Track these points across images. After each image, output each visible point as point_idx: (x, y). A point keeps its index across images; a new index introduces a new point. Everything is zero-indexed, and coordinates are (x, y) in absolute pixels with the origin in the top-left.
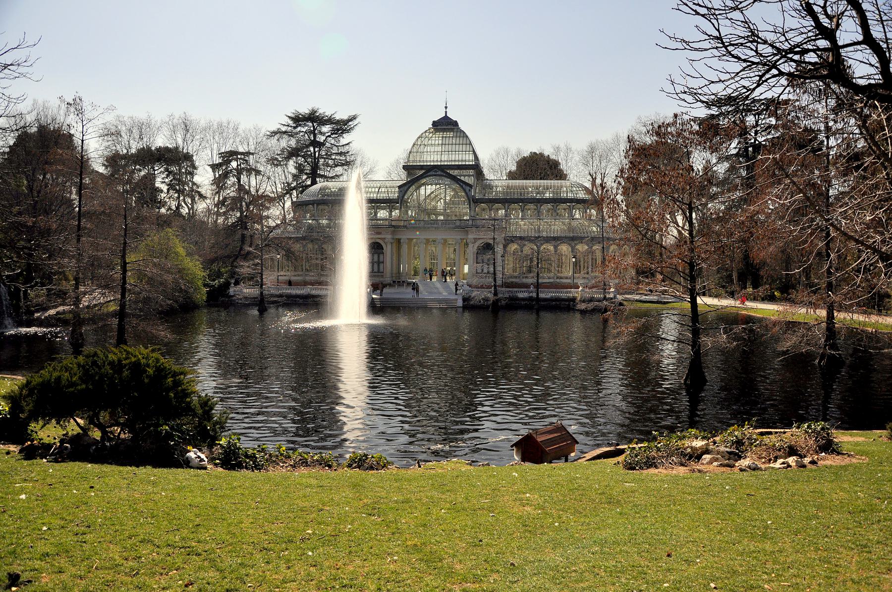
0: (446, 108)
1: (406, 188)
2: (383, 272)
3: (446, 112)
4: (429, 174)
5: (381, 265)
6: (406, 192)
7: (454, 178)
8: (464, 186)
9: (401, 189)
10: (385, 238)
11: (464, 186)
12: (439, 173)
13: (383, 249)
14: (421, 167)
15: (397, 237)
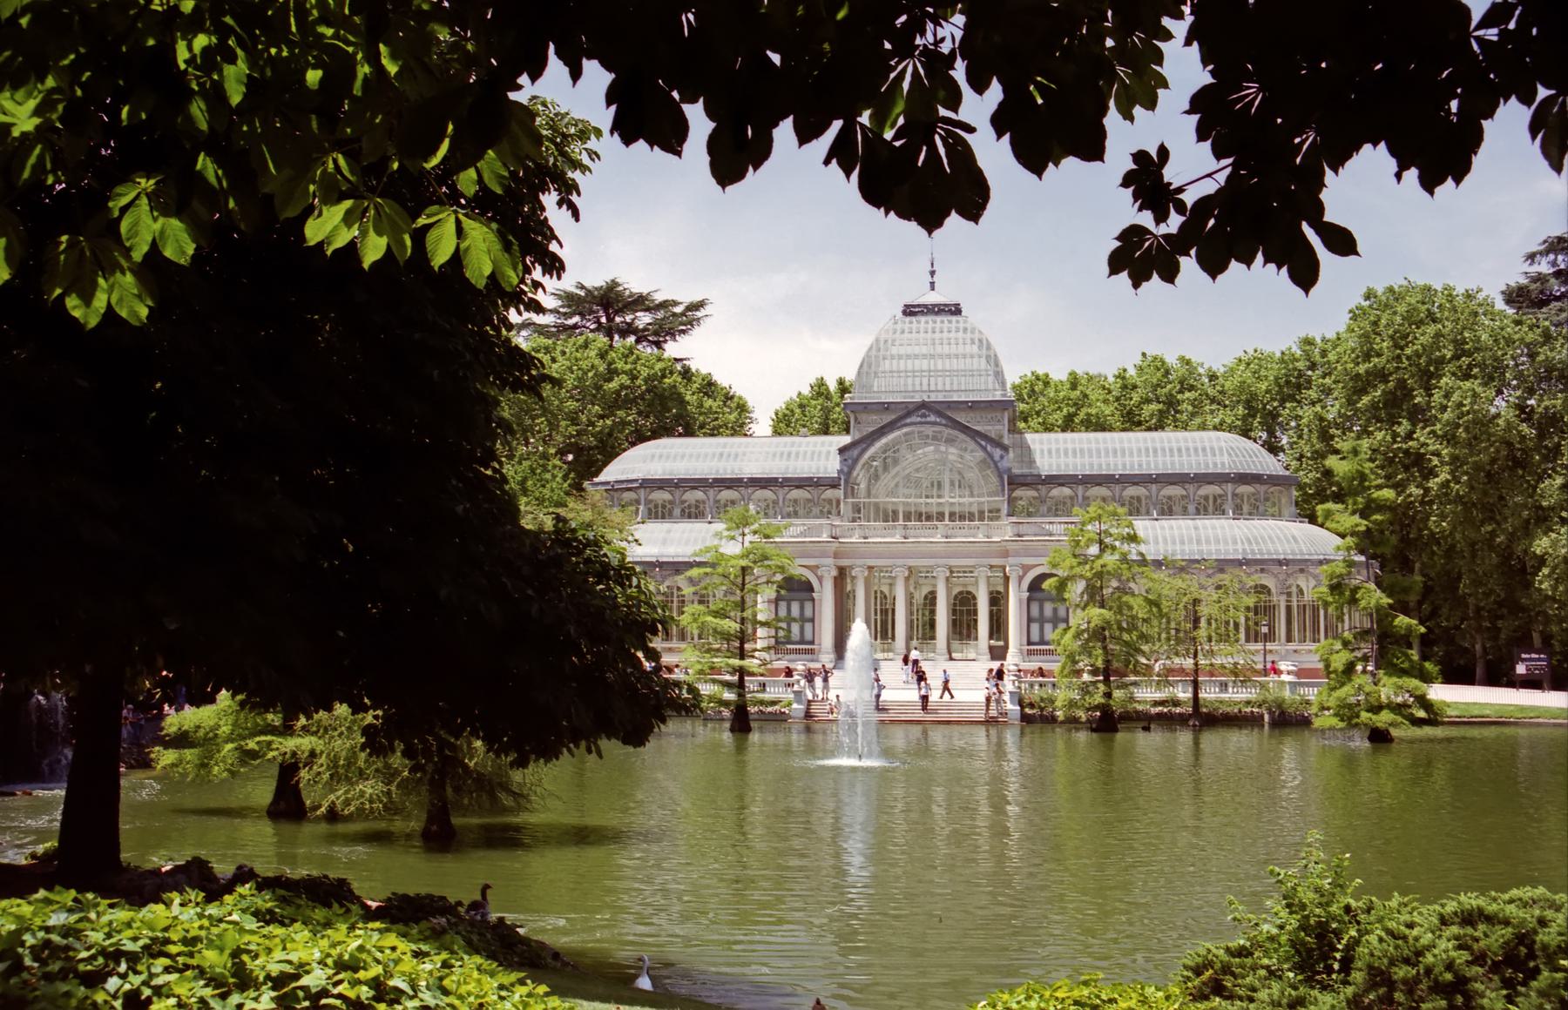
0: (933, 273)
1: (856, 452)
2: (812, 643)
3: (932, 284)
4: (908, 421)
5: (808, 626)
6: (856, 461)
7: (965, 429)
8: (989, 448)
9: (847, 455)
10: (817, 567)
11: (989, 448)
12: (932, 418)
13: (812, 590)
14: (886, 407)
15: (845, 562)
